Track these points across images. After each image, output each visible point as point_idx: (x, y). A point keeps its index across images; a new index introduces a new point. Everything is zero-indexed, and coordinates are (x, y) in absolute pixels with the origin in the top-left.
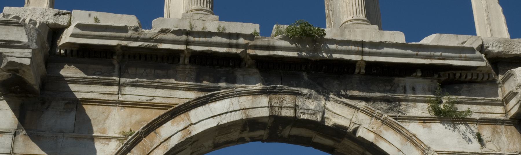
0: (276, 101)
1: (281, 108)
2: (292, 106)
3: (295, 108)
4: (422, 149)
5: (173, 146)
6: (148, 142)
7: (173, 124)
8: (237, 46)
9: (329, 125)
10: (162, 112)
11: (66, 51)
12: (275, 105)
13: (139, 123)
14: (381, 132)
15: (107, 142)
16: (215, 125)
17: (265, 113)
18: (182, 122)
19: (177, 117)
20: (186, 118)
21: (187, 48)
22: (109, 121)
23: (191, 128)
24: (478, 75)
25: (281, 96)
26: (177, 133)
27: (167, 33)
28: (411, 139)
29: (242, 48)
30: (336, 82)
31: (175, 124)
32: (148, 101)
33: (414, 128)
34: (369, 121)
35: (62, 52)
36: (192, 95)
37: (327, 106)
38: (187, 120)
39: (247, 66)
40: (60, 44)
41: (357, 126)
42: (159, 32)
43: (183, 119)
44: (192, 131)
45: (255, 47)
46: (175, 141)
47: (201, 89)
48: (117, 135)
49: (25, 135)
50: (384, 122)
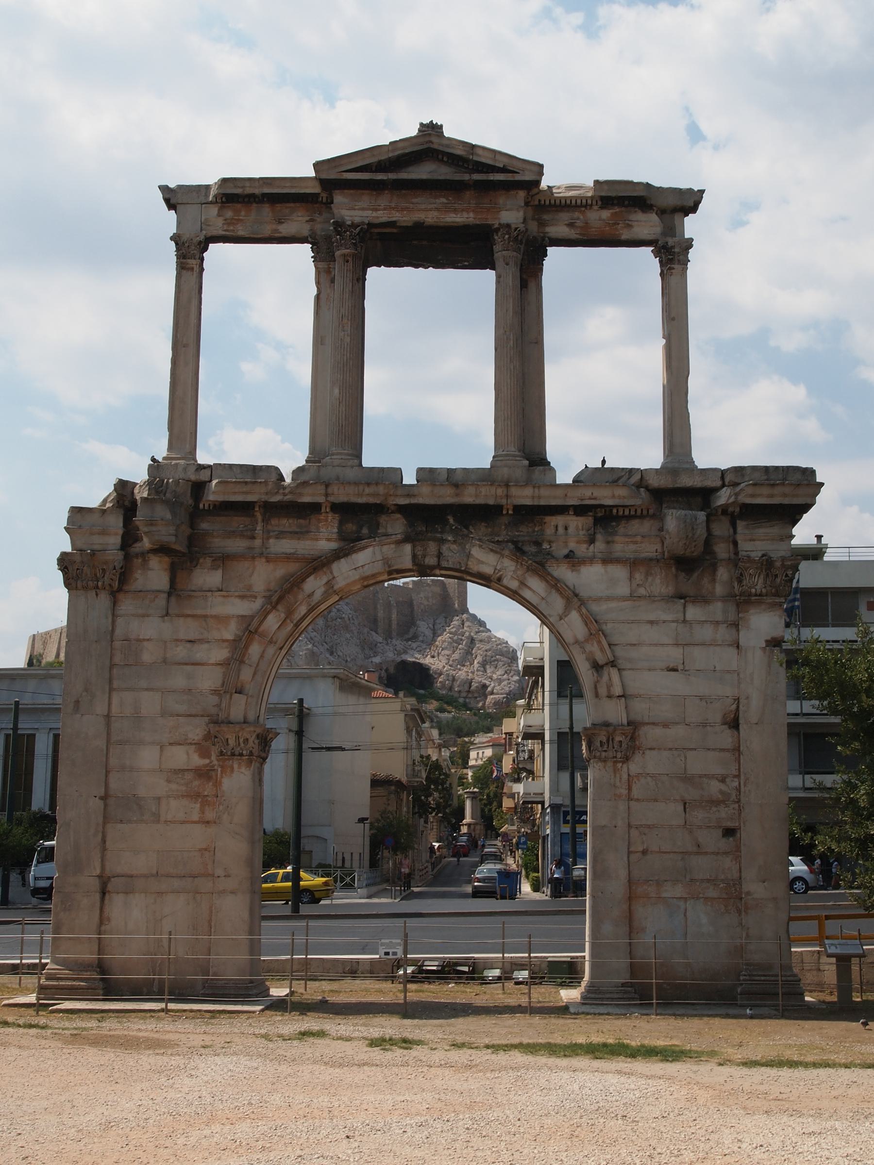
0: (420, 548)
1: (424, 556)
3: (439, 555)
7: (316, 578)
14: (525, 578)
16: (357, 577)
21: (327, 501)
24: (636, 510)
30: (483, 524)
33: (562, 572)
34: (513, 568)
36: (334, 545)
37: (471, 552)
43: (325, 573)
46: (318, 596)
50: (528, 569)
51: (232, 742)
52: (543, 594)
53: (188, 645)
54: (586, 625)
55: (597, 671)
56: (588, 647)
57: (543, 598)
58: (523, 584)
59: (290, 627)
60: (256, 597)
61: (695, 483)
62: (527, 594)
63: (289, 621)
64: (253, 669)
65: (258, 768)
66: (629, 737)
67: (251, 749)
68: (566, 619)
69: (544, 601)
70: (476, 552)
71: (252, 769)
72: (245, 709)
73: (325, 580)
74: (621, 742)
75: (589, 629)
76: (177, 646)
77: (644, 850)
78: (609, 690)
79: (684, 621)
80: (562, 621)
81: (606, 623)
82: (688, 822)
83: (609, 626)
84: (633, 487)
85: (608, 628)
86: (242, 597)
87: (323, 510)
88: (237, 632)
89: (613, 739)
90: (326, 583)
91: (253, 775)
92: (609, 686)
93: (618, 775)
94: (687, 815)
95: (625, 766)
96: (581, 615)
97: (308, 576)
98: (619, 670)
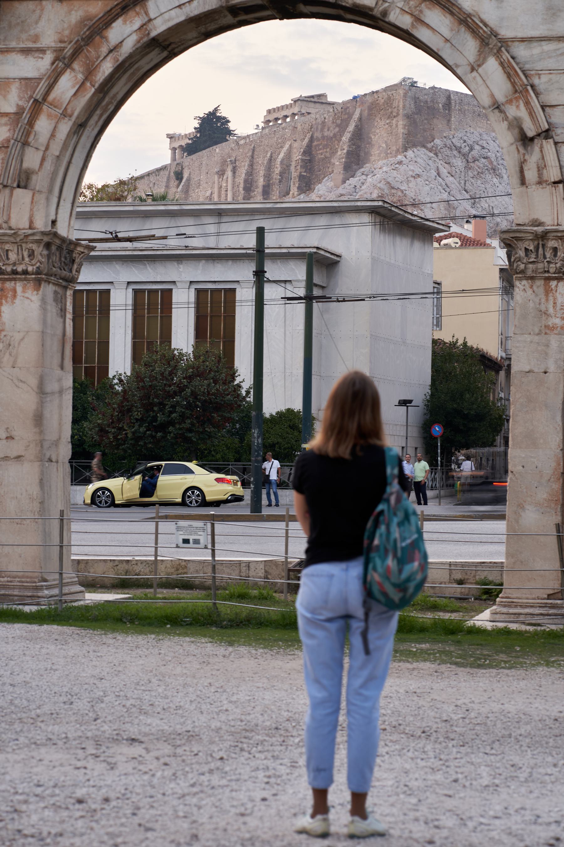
4: (480, 37)
5: (127, 55)
6: (93, 53)
7: (125, 22)
9: (348, 5)
13: (82, 22)
14: (421, 11)
15: (41, 56)
16: (182, 18)
18: (136, 18)
20: (143, 12)
22: (42, 23)
23: (150, 26)
26: (131, 34)
31: (128, 22)
38: (144, 15)
41: (387, 4)
43: (138, 14)
44: (151, 30)
46: (128, 47)
48: (53, 44)
51: (13, 256)
52: (446, 33)
54: (509, 76)
55: (525, 145)
56: (512, 111)
57: (447, 40)
58: (418, 20)
60: (42, 51)
62: (423, 34)
63: (88, 84)
64: (40, 154)
65: (56, 292)
67: (38, 264)
68: (480, 70)
69: (448, 45)
71: (40, 292)
72: (31, 210)
73: (137, 23)
74: (555, 250)
75: (513, 84)
78: (540, 175)
80: (475, 74)
81: (539, 75)
83: (544, 78)
85: (541, 82)
86: (26, 51)
88: (21, 103)
89: (543, 246)
90: (139, 29)
91: (43, 301)
92: (541, 168)
93: (551, 298)
96: (502, 64)
97: (114, 19)
98: (556, 143)
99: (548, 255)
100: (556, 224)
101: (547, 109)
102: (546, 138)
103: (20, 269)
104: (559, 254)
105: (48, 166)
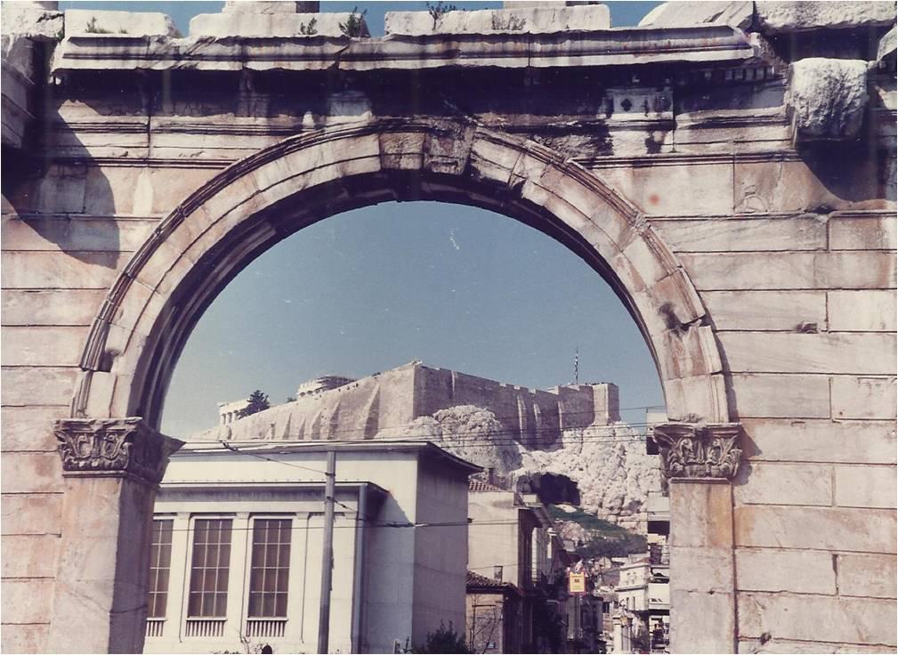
1: (399, 155)
2: (417, 150)
8: (323, 57)
10: (215, 173)
11: (63, 80)
12: (390, 152)
17: (372, 166)
19: (236, 181)
23: (258, 198)
25: (401, 135)
27: (210, 43)
28: (608, 198)
29: (331, 60)
32: (194, 157)
34: (540, 172)
35: (58, 81)
36: (262, 143)
37: (474, 149)
39: (346, 86)
40: (53, 70)
41: (521, 180)
42: (198, 42)
45: (352, 58)
47: (273, 132)
49: (13, 219)
53: (27, 297)
54: (660, 259)
59: (187, 266)
61: (848, 19)
62: (562, 213)
65: (135, 492)
66: (730, 442)
70: (484, 149)
76: (10, 299)
77: (764, 635)
79: (826, 250)
82: (842, 592)
84: (740, 31)
87: (242, 87)
94: (840, 573)
95: (726, 489)
97: (217, 190)
98: (715, 331)
99: (709, 456)
100: (717, 419)
101: (701, 293)
102: (704, 324)
103: (95, 464)
104: (722, 454)
105: (137, 350)
